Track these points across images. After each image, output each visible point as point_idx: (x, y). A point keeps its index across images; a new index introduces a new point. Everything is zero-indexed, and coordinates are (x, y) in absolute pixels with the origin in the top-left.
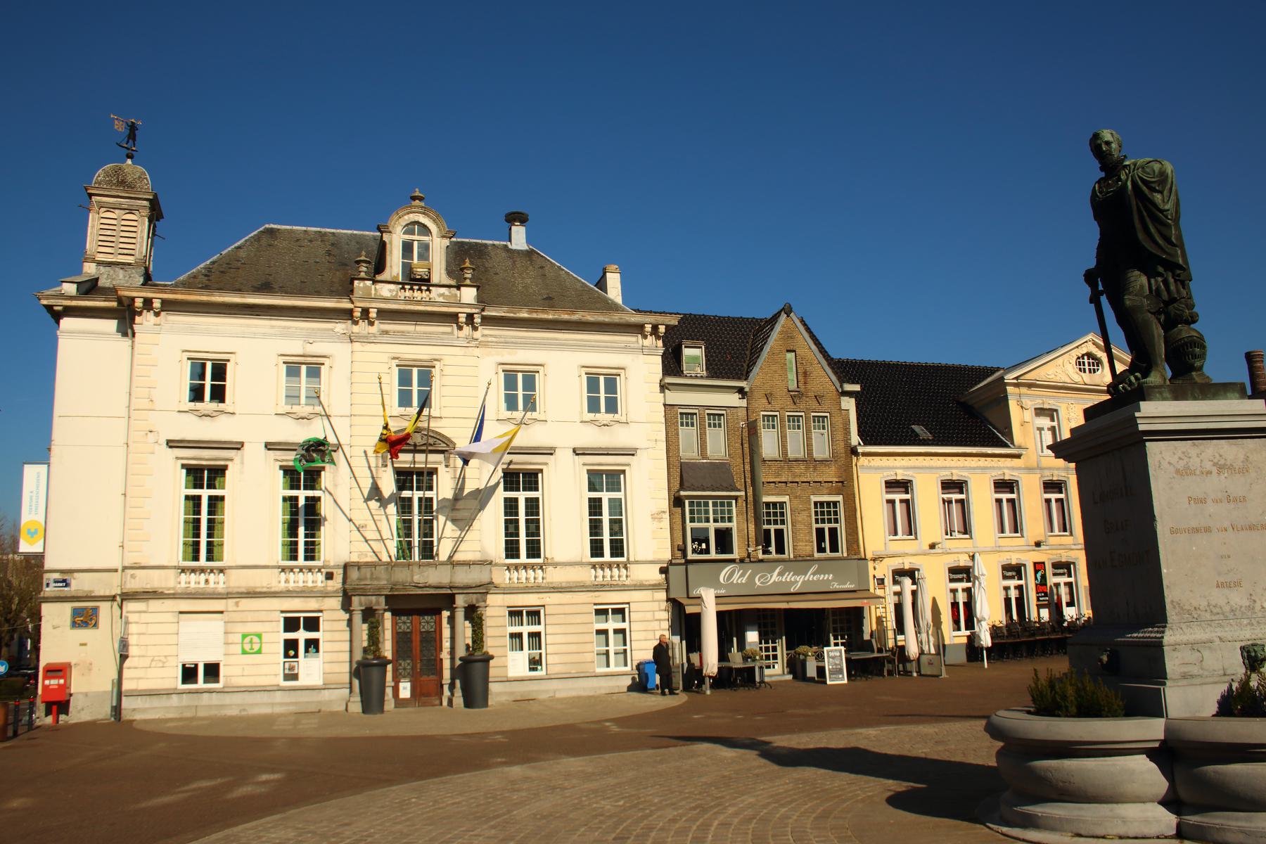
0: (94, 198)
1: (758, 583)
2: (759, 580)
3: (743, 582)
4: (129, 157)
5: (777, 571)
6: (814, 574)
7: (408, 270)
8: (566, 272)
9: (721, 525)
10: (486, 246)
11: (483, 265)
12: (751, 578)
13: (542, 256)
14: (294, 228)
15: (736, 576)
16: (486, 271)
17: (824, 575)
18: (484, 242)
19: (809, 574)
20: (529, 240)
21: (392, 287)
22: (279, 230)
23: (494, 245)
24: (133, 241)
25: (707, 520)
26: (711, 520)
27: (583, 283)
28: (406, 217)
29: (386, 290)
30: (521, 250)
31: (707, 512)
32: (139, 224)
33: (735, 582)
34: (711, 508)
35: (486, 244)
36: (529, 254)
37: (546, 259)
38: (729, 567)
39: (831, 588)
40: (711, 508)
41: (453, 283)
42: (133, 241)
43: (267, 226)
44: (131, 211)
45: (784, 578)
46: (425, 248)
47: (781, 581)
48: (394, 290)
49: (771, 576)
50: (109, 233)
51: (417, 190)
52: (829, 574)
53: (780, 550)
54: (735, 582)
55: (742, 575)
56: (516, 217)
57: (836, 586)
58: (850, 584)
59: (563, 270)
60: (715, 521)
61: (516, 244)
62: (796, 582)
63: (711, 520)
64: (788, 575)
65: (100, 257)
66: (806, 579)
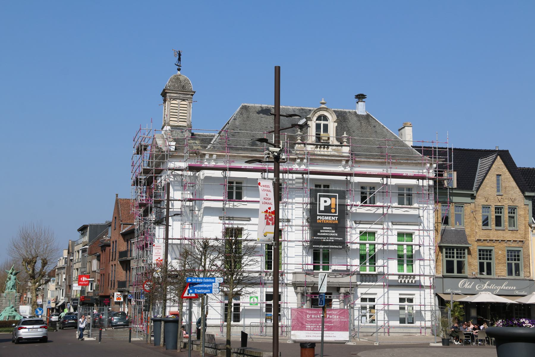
0: (168, 95)
1: (477, 289)
2: (478, 287)
3: (470, 287)
4: (179, 70)
5: (487, 283)
6: (506, 286)
7: (318, 138)
8: (386, 129)
9: (459, 259)
10: (345, 112)
11: (347, 126)
12: (474, 286)
13: (374, 119)
14: (256, 105)
15: (466, 286)
16: (349, 130)
17: (511, 287)
18: (345, 110)
19: (503, 286)
20: (367, 109)
21: (312, 146)
22: (249, 106)
23: (350, 112)
24: (185, 115)
25: (453, 257)
26: (455, 257)
27: (395, 136)
28: (318, 113)
29: (309, 148)
30: (363, 115)
31: (453, 253)
32: (188, 106)
33: (466, 287)
34: (455, 251)
35: (346, 111)
36: (368, 117)
37: (376, 120)
38: (463, 280)
39: (515, 294)
40: (455, 251)
41: (339, 144)
42: (185, 115)
43: (243, 104)
44: (184, 100)
45: (491, 287)
46: (326, 127)
47: (489, 288)
48: (313, 148)
49: (484, 286)
50: (174, 111)
51: (323, 99)
52: (514, 287)
53: (489, 273)
54: (466, 287)
55: (470, 284)
56: (361, 97)
57: (517, 293)
58: (524, 292)
59: (385, 128)
60: (457, 257)
61: (361, 112)
62: (497, 289)
63: (455, 257)
64: (492, 286)
65: (172, 123)
66: (502, 288)
